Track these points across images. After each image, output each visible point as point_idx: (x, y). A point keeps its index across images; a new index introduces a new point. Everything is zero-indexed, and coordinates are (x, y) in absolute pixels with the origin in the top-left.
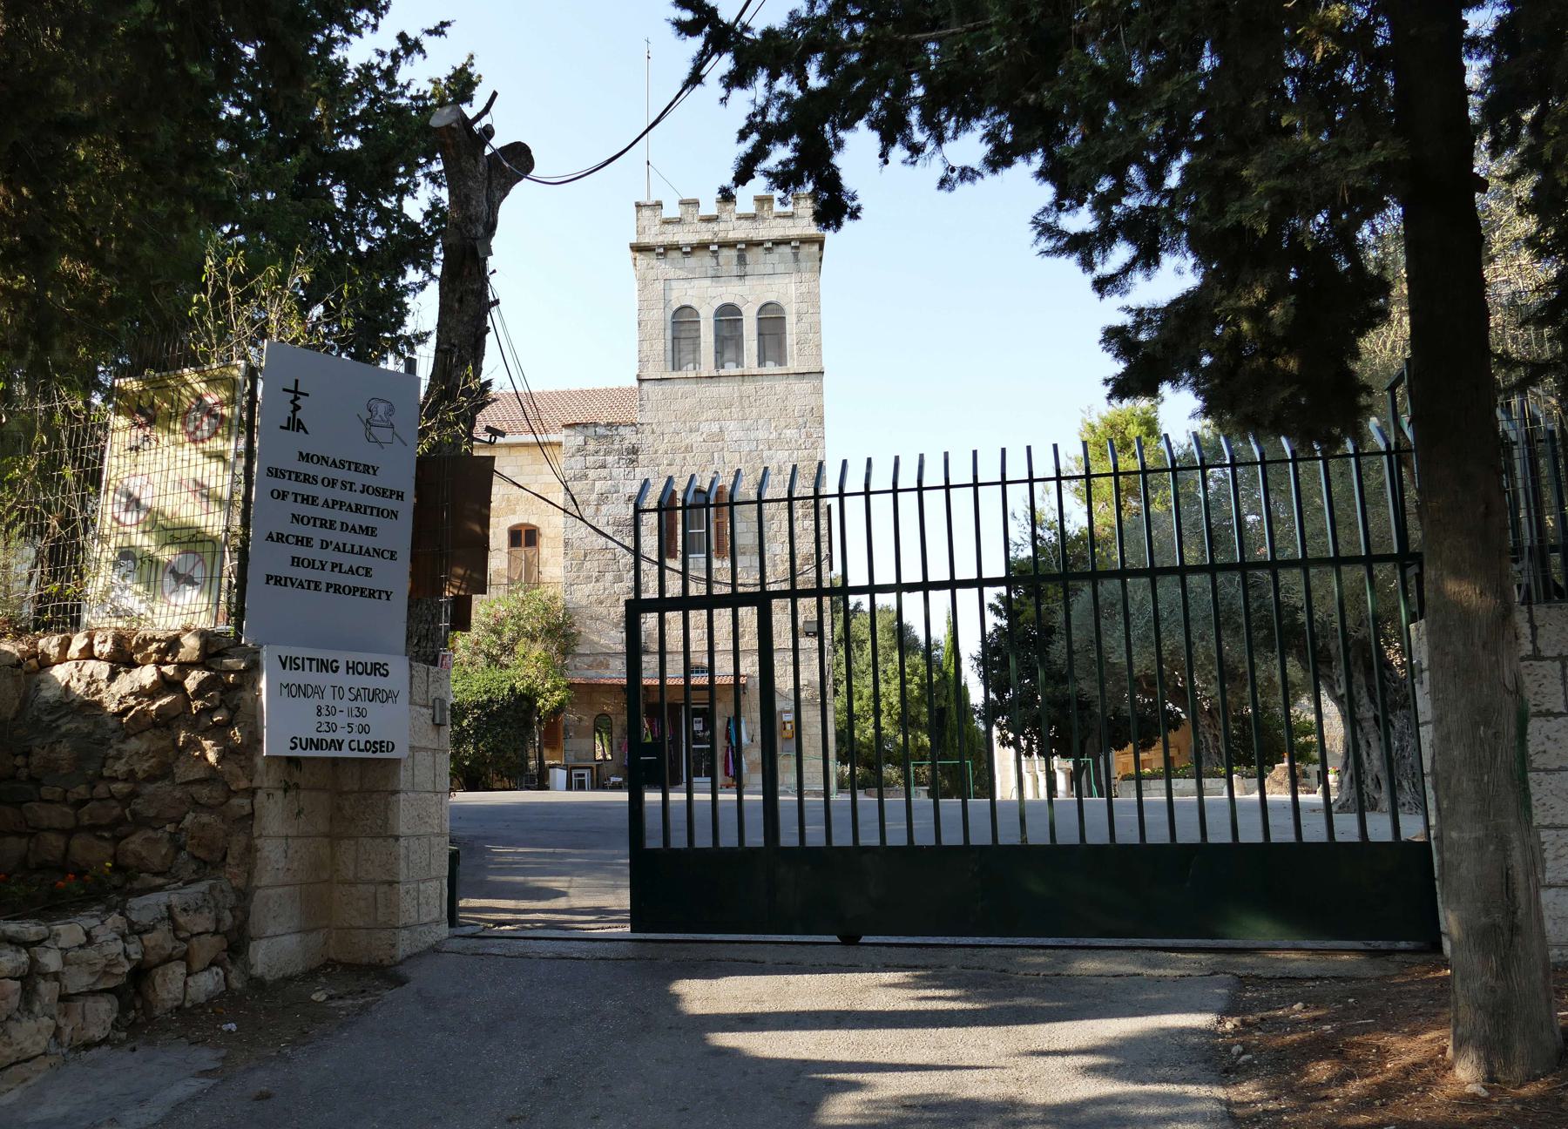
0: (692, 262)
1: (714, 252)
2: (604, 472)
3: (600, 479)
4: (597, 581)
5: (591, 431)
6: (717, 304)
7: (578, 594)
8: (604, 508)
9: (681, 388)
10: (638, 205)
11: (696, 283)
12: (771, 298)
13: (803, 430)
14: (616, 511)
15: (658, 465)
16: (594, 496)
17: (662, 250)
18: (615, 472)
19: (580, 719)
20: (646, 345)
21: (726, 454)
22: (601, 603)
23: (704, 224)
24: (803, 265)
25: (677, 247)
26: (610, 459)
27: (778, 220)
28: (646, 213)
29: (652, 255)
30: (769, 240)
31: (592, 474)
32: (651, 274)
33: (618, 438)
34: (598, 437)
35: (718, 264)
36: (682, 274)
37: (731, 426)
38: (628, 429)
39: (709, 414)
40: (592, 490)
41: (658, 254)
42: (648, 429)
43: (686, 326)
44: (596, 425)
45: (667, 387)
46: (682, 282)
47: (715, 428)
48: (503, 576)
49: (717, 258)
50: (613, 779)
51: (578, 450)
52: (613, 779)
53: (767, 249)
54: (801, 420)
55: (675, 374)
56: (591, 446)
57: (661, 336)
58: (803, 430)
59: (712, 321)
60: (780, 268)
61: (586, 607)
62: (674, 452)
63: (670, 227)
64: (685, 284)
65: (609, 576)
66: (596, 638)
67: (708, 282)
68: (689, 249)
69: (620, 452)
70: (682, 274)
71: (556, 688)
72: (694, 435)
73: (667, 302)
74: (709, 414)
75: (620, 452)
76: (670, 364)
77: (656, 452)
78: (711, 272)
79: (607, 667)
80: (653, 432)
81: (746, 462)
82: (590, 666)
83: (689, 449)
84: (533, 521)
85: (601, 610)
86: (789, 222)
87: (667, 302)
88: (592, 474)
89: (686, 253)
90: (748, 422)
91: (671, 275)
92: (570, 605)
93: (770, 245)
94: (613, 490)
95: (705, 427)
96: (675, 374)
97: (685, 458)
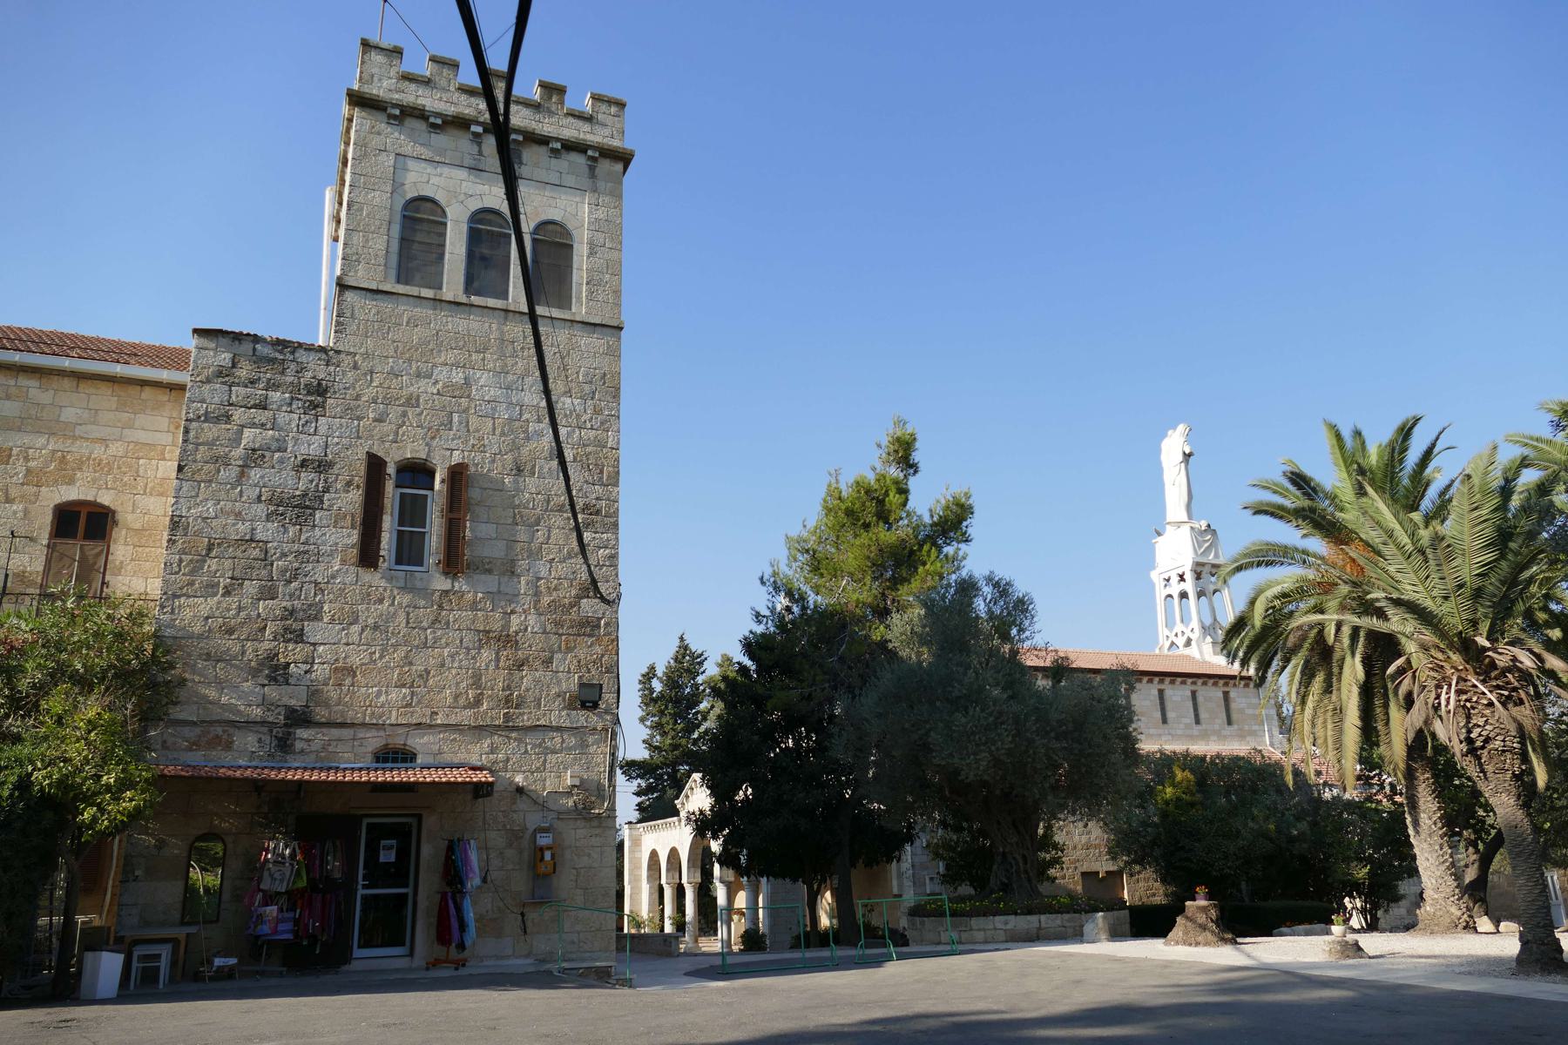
0: (440, 140)
1: (476, 135)
2: (261, 416)
3: (253, 425)
4: (227, 593)
5: (247, 347)
6: (475, 205)
7: (188, 614)
8: (255, 474)
9: (406, 311)
10: (366, 45)
11: (446, 170)
12: (555, 215)
13: (590, 402)
14: (276, 480)
15: (359, 419)
16: (239, 452)
17: (397, 112)
18: (282, 418)
19: (161, 844)
20: (358, 239)
21: (474, 422)
22: (230, 631)
23: (464, 97)
24: (601, 185)
25: (420, 114)
26: (275, 396)
27: (571, 120)
28: (377, 58)
29: (382, 117)
30: (557, 139)
31: (238, 415)
32: (376, 141)
33: (293, 366)
34: (259, 360)
35: (480, 153)
36: (426, 153)
37: (484, 378)
38: (312, 356)
39: (450, 357)
40: (238, 440)
41: (390, 116)
42: (347, 361)
43: (425, 227)
44: (256, 339)
45: (387, 306)
46: (423, 165)
47: (458, 377)
48: (32, 583)
49: (479, 144)
50: (218, 962)
51: (219, 374)
52: (218, 962)
53: (554, 151)
54: (587, 388)
55: (401, 289)
56: (243, 372)
57: (384, 230)
58: (590, 402)
59: (465, 228)
60: (570, 180)
61: (200, 637)
62: (388, 402)
63: (413, 86)
64: (429, 169)
65: (251, 588)
66: (212, 693)
67: (462, 174)
68: (439, 121)
69: (295, 388)
70: (426, 153)
71: (125, 784)
72: (423, 382)
73: (397, 187)
74: (450, 357)
75: (295, 388)
76: (393, 273)
77: (358, 397)
78: (468, 161)
79: (228, 746)
80: (355, 367)
81: (503, 434)
82: (194, 745)
83: (413, 401)
84: (105, 499)
85: (231, 645)
86: (586, 127)
87: (397, 187)
88: (238, 415)
89: (434, 126)
90: (510, 378)
91: (408, 148)
92: (168, 632)
93: (558, 146)
94: (274, 446)
95: (441, 374)
96: (401, 289)
97: (404, 414)
